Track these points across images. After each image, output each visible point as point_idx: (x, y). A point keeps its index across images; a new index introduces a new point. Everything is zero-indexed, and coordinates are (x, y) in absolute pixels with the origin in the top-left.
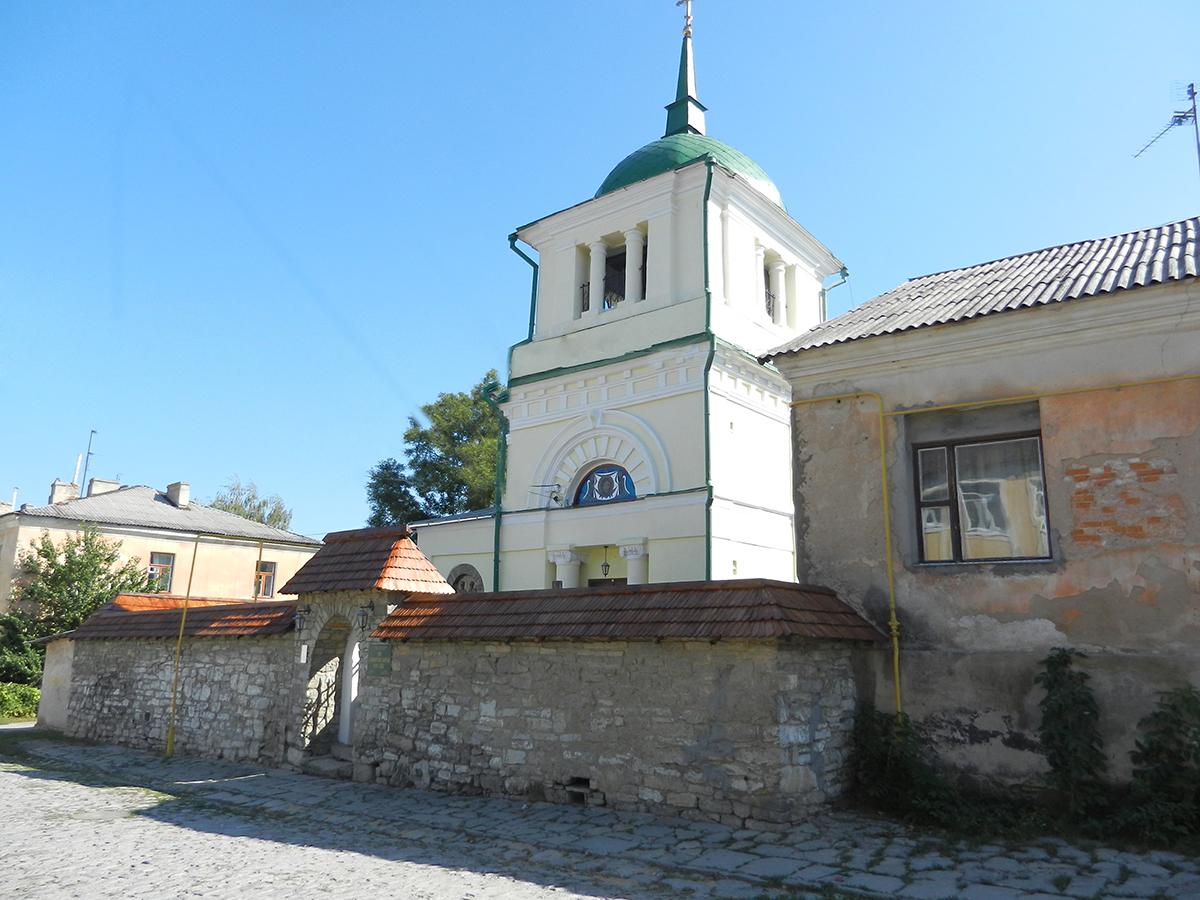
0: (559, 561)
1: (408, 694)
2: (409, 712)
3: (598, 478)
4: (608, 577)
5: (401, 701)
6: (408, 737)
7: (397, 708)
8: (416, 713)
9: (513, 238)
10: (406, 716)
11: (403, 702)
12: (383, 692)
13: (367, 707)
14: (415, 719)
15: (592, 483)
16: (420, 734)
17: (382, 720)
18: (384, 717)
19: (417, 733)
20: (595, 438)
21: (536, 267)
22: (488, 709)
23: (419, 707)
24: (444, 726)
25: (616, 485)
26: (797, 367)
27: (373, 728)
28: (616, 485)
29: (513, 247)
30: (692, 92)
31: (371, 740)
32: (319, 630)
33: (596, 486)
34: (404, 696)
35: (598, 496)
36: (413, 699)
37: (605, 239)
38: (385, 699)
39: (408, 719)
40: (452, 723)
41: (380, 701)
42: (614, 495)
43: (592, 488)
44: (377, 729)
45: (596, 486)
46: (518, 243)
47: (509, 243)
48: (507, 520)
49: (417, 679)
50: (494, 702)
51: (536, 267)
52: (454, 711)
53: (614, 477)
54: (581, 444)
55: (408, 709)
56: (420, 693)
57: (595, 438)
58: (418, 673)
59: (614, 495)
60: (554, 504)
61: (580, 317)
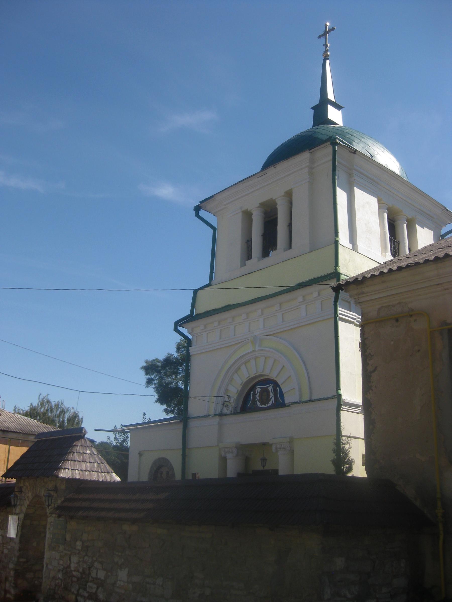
0: (229, 456)
1: (75, 559)
2: (75, 573)
3: (259, 390)
4: (266, 468)
5: (70, 564)
9: (197, 209)
10: (73, 576)
15: (254, 394)
16: (81, 591)
17: (59, 578)
18: (60, 575)
19: (78, 591)
20: (255, 358)
21: (214, 229)
22: (123, 574)
23: (81, 570)
24: (95, 586)
25: (272, 395)
26: (363, 293)
28: (272, 395)
29: (197, 215)
30: (331, 96)
32: (26, 506)
33: (257, 396)
34: (72, 560)
35: (259, 404)
37: (262, 205)
38: (61, 562)
40: (100, 584)
42: (271, 403)
43: (254, 398)
44: (56, 585)
45: (257, 396)
46: (202, 213)
47: (194, 212)
48: (192, 424)
50: (127, 570)
51: (214, 229)
52: (101, 575)
53: (270, 388)
54: (245, 363)
55: (75, 571)
56: (81, 560)
57: (255, 358)
59: (271, 403)
60: (225, 411)
61: (245, 265)
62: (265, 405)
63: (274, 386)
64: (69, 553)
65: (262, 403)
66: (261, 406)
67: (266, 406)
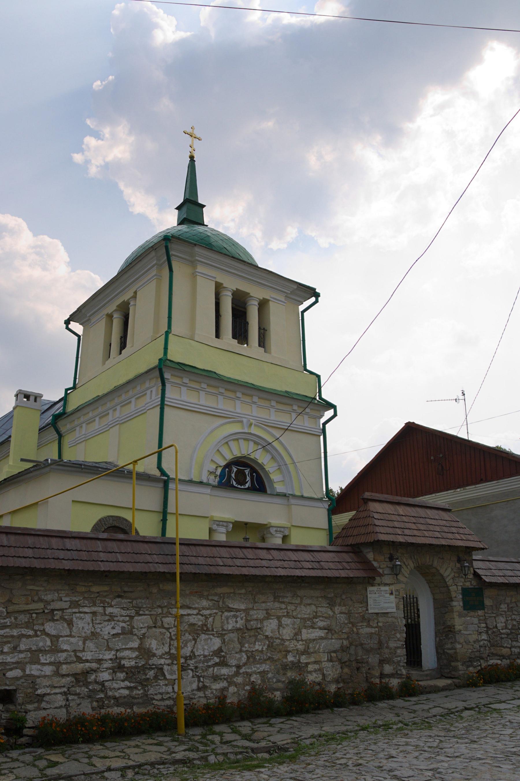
3: (235, 470)
6: (506, 647)
7: (494, 630)
8: (509, 631)
10: (502, 634)
11: (498, 625)
12: (479, 620)
13: (468, 633)
14: (508, 634)
18: (484, 637)
23: (510, 627)
25: (248, 478)
27: (477, 646)
28: (248, 478)
31: (477, 654)
35: (234, 483)
36: (505, 622)
39: (503, 636)
41: (478, 626)
42: (247, 485)
43: (230, 477)
49: (506, 610)
53: (247, 472)
55: (502, 629)
56: (510, 618)
58: (506, 605)
59: (247, 485)
62: (241, 485)
63: (250, 470)
64: (494, 615)
65: (238, 483)
66: (236, 486)
67: (243, 487)
